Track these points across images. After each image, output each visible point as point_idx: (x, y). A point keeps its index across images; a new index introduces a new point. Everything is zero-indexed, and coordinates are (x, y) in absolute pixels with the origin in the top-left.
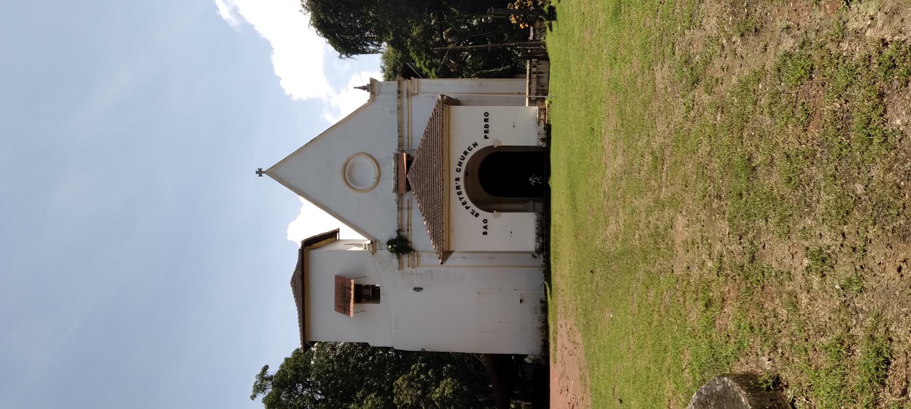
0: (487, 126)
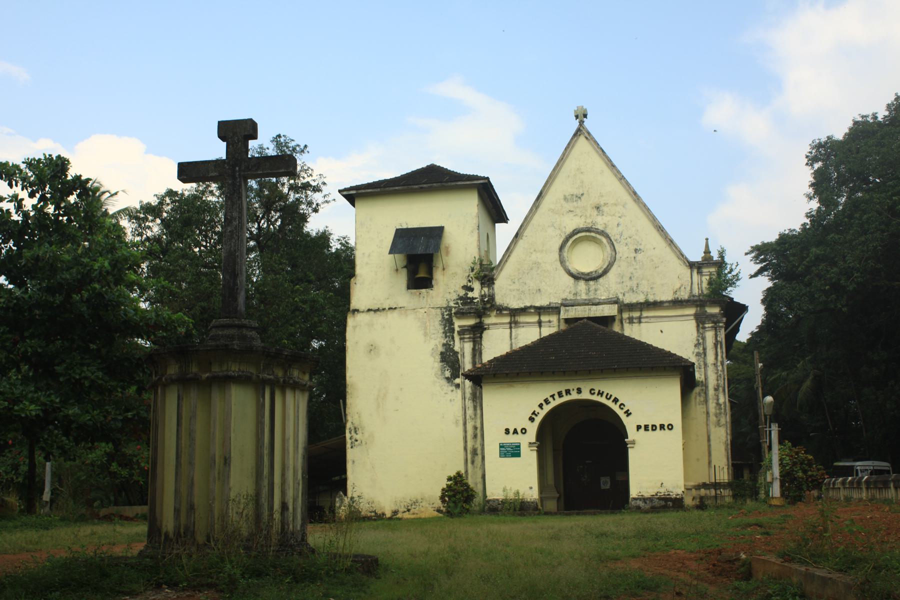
0: (654, 428)
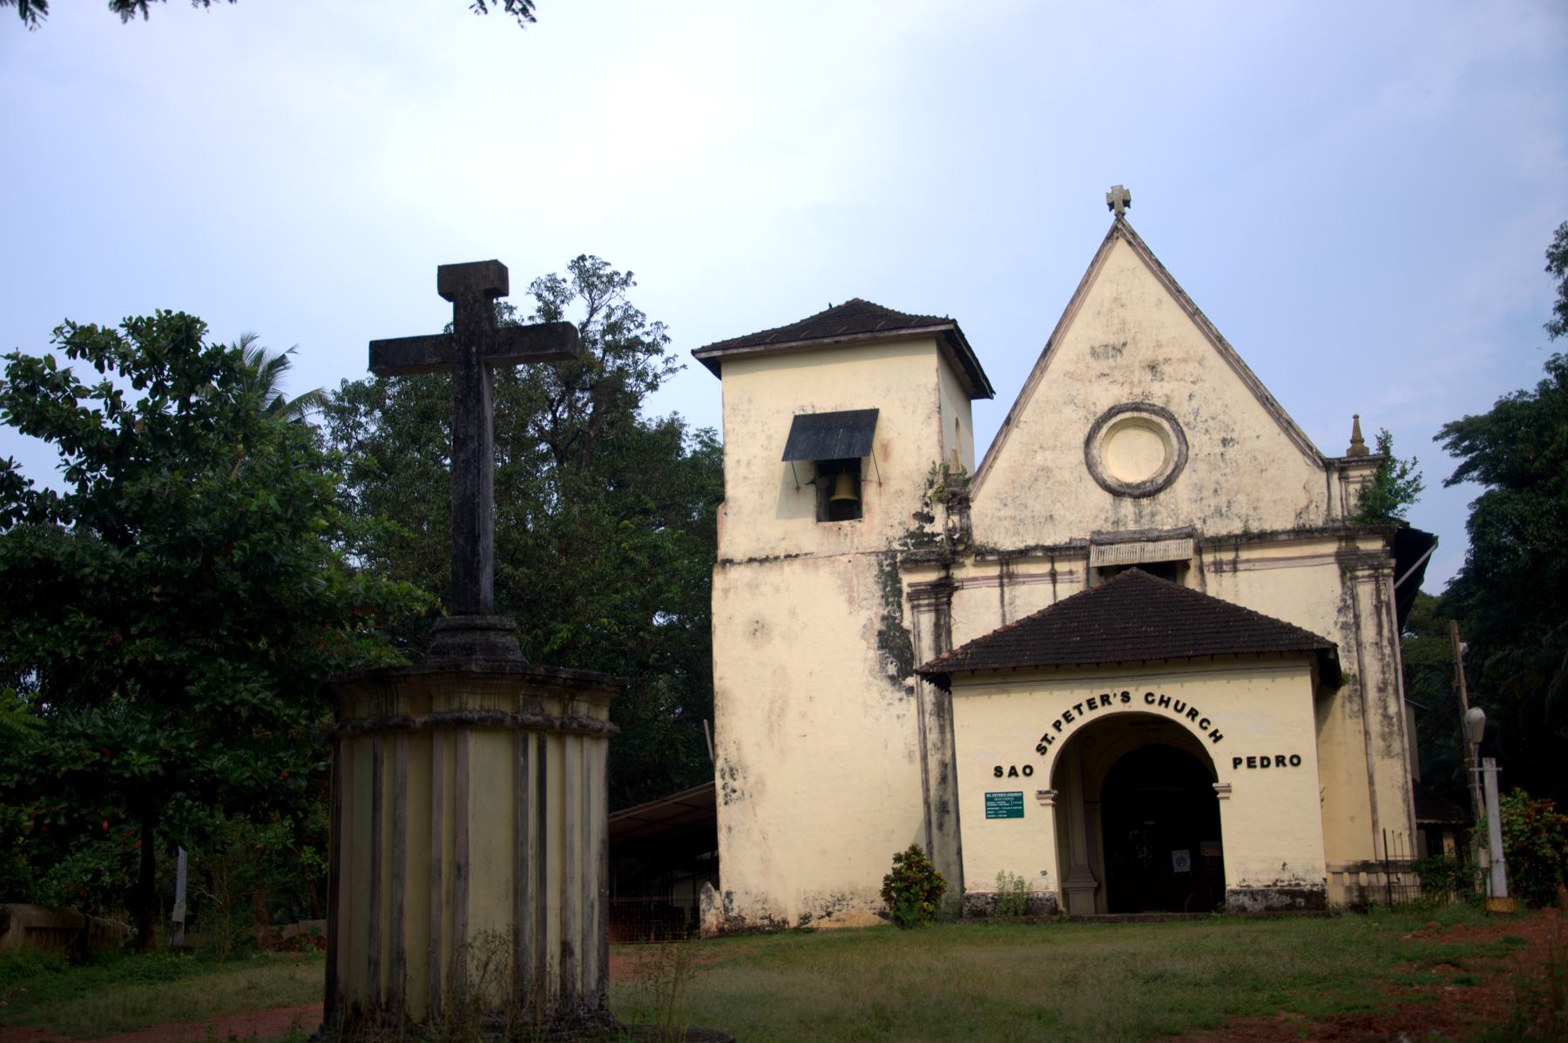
0: (1265, 763)
